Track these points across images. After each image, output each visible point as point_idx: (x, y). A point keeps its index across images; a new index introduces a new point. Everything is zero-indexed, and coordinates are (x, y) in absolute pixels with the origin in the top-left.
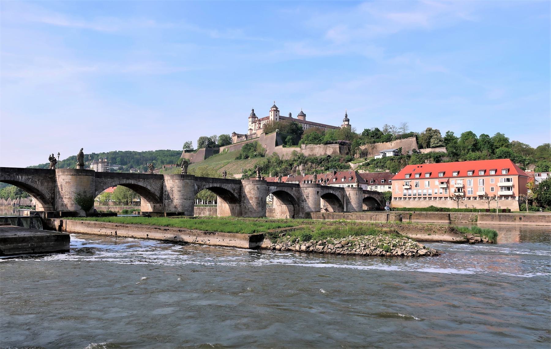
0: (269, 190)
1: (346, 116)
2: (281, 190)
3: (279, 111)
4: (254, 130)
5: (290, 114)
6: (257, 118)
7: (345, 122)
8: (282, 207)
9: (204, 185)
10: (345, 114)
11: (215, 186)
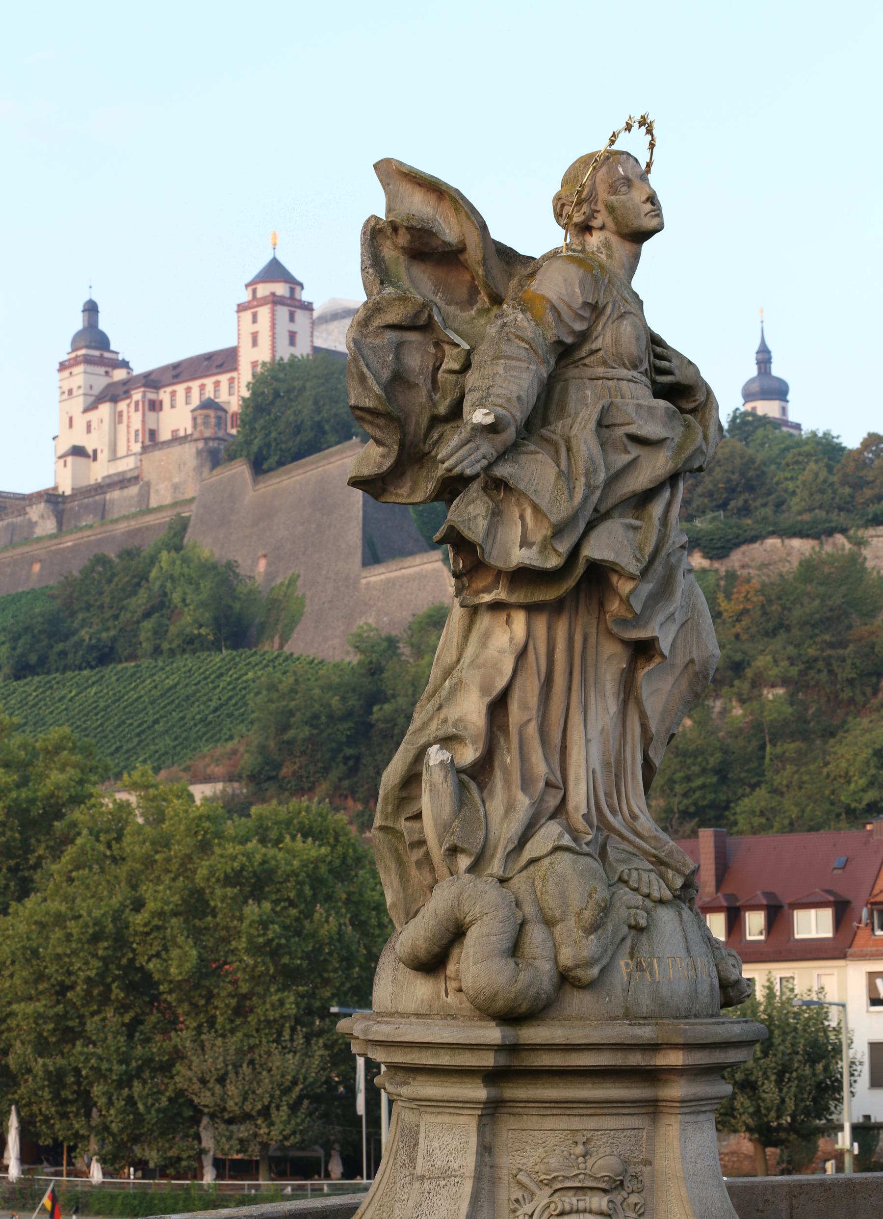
1: (764, 358)
4: (103, 457)
6: (125, 364)
10: (756, 346)
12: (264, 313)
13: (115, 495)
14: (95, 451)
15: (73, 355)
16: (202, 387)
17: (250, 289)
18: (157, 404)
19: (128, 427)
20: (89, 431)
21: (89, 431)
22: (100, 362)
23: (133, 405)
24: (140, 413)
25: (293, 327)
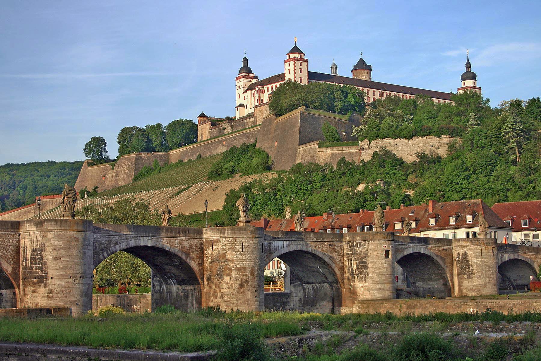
0: (270, 250)
1: (468, 65)
2: (299, 249)
3: (306, 61)
5: (335, 68)
6: (256, 78)
7: (466, 81)
8: (304, 289)
9: (116, 244)
11: (143, 244)
12: (292, 63)
13: (248, 120)
14: (246, 105)
15: (240, 75)
16: (272, 87)
17: (288, 56)
18: (263, 91)
19: (255, 98)
20: (245, 99)
21: (245, 99)
22: (248, 77)
23: (256, 91)
24: (258, 94)
25: (301, 67)
